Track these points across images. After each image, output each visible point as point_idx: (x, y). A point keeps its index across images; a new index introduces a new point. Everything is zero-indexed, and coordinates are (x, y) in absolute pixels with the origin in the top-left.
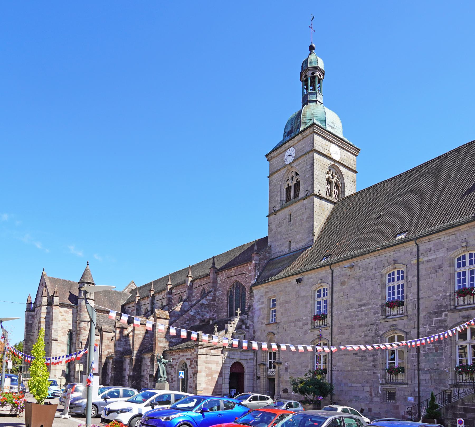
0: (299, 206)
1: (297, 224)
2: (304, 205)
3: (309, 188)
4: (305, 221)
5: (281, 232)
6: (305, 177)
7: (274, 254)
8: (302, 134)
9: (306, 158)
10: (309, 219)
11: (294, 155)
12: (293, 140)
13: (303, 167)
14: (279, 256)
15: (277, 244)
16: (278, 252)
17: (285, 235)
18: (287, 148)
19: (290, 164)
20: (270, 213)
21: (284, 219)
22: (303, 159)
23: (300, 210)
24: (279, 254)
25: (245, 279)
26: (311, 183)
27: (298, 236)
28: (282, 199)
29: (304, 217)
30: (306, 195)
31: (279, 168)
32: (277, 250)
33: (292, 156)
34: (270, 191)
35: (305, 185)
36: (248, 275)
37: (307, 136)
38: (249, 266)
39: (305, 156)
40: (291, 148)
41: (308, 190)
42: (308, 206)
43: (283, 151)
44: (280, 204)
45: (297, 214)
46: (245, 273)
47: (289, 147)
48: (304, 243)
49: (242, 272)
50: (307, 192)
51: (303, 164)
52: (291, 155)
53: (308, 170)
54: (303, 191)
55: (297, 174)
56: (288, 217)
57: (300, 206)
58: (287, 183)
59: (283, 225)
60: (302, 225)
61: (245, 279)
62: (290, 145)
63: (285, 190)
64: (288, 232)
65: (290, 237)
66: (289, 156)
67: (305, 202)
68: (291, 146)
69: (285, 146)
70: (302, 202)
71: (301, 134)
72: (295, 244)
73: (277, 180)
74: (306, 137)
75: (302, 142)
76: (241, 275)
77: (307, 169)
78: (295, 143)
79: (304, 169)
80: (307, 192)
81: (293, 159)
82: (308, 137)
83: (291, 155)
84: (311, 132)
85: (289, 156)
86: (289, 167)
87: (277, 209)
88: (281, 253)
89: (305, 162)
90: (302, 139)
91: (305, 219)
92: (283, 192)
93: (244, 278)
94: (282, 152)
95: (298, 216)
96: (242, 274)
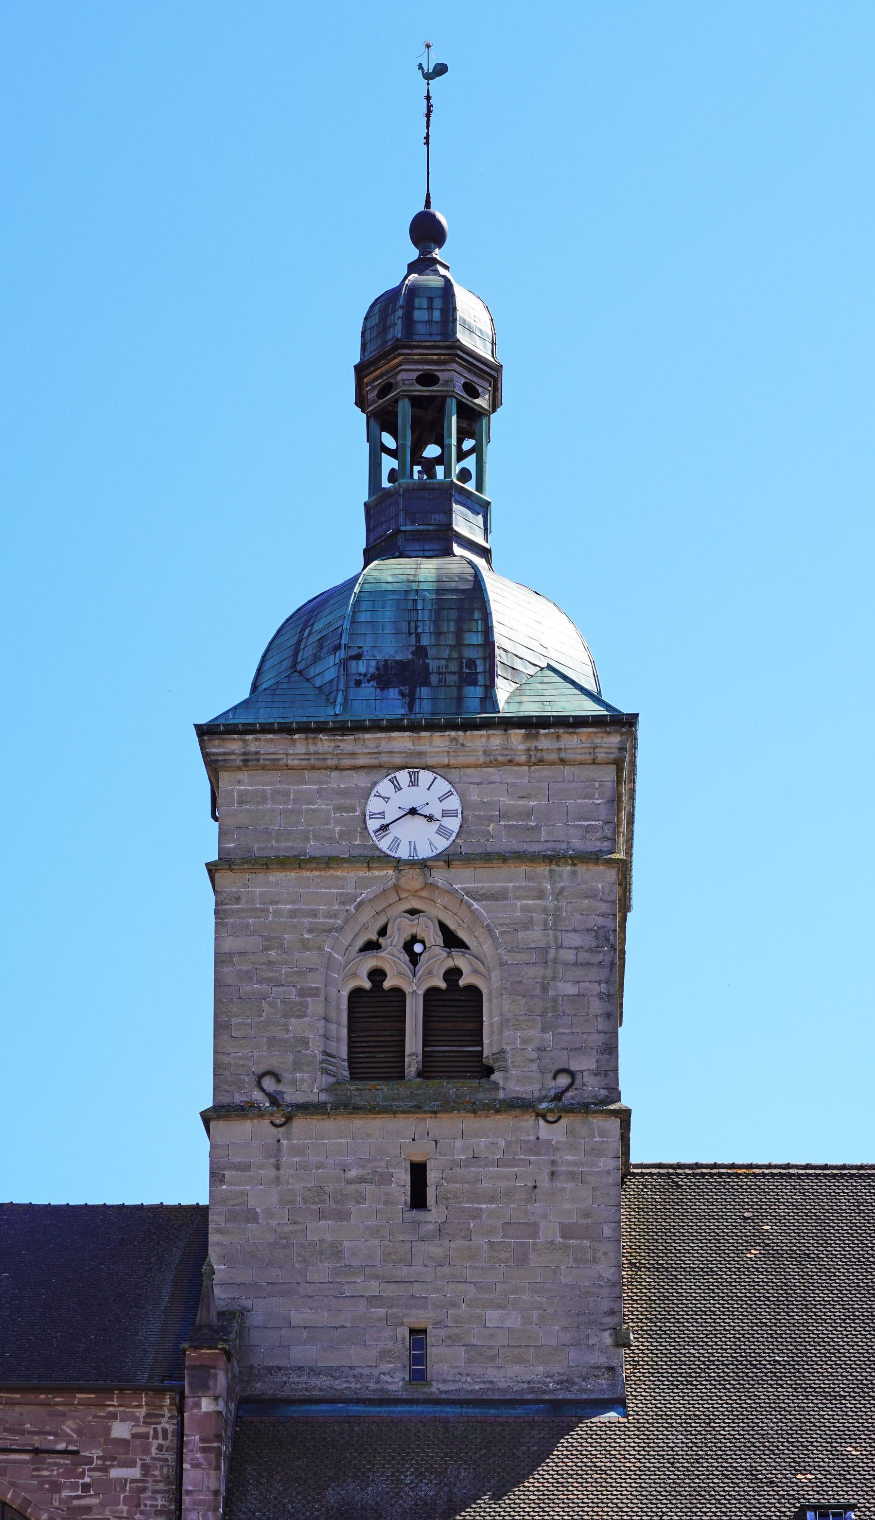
0: (502, 1143)
1: (481, 1241)
2: (538, 1146)
3: (584, 1064)
4: (552, 1243)
5: (337, 1253)
6: (545, 989)
7: (270, 1369)
8: (536, 736)
9: (553, 882)
10: (586, 1242)
11: (453, 824)
12: (455, 739)
13: (527, 925)
14: (316, 1394)
15: (296, 1318)
16: (314, 1371)
17: (376, 1277)
18: (398, 760)
19: (424, 865)
20: (225, 1100)
21: (362, 1180)
22: (528, 878)
23: (499, 1163)
24: (322, 1382)
25: (65, 1493)
26: (600, 1039)
27: (493, 1317)
28: (332, 1047)
29: (545, 1216)
30: (558, 1097)
31: (312, 847)
32: (300, 1354)
33: (435, 826)
34: (221, 959)
35: (548, 1036)
36: (105, 1469)
37: (563, 762)
38: (113, 1416)
39: (543, 869)
40: (425, 777)
41: (572, 1074)
42: (574, 1164)
43: (361, 761)
44: (325, 1072)
45: (484, 1185)
46: (76, 1453)
47: (416, 761)
48: (541, 1369)
49: (37, 1441)
50: (564, 1081)
51: (525, 909)
52: (430, 818)
53: (568, 956)
54: (534, 1066)
55: (452, 941)
56: (404, 1177)
57: (509, 1144)
58: (370, 962)
59: (351, 1206)
60: (523, 1260)
61: (65, 1493)
62: (420, 754)
63: (345, 993)
64: (404, 1271)
65: (422, 1302)
66: (413, 812)
67: (544, 1130)
68: (431, 761)
69: (384, 746)
70: (523, 1124)
71: (527, 737)
72: (469, 1361)
73: (293, 914)
74: (552, 764)
75: (521, 776)
76: (26, 1457)
77: (560, 947)
78: (461, 760)
79: (535, 936)
80: (564, 1081)
81: (442, 844)
82: (567, 770)
83: (430, 818)
84: (601, 756)
85: (413, 812)
86: (412, 879)
87: (291, 1096)
88: (340, 1385)
89: (549, 902)
90: (529, 763)
91: (549, 1231)
92: (339, 1009)
93: (56, 1487)
94: (347, 762)
95: (492, 1199)
96: (36, 1451)
